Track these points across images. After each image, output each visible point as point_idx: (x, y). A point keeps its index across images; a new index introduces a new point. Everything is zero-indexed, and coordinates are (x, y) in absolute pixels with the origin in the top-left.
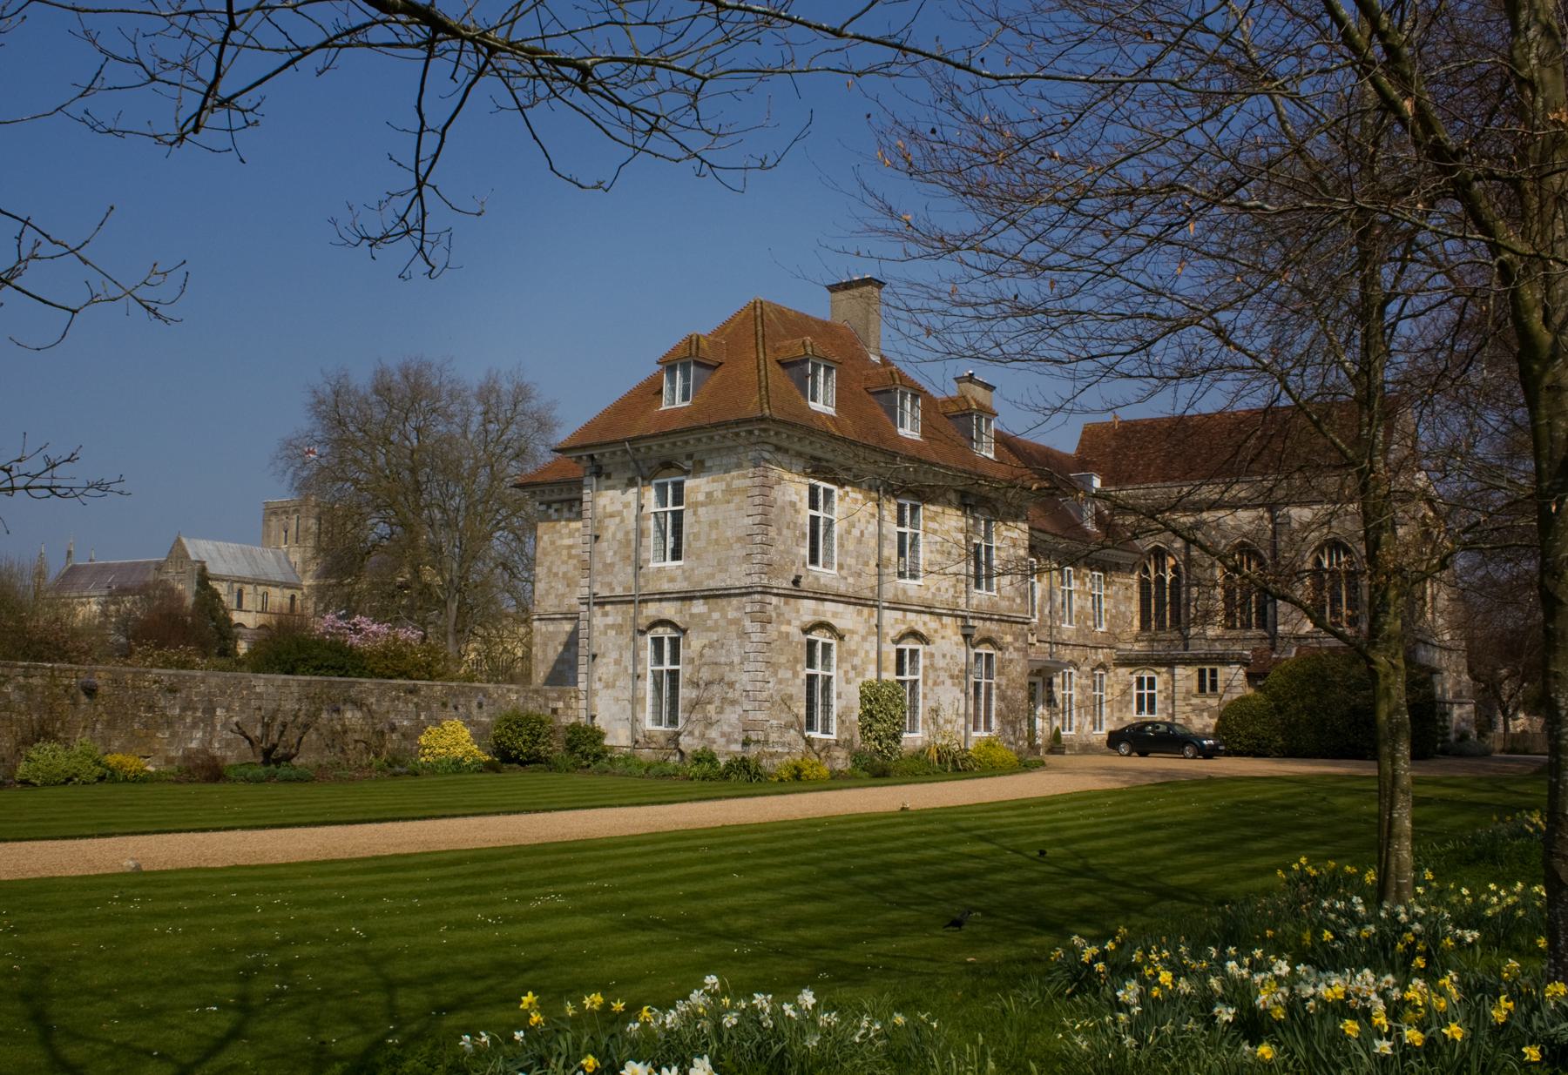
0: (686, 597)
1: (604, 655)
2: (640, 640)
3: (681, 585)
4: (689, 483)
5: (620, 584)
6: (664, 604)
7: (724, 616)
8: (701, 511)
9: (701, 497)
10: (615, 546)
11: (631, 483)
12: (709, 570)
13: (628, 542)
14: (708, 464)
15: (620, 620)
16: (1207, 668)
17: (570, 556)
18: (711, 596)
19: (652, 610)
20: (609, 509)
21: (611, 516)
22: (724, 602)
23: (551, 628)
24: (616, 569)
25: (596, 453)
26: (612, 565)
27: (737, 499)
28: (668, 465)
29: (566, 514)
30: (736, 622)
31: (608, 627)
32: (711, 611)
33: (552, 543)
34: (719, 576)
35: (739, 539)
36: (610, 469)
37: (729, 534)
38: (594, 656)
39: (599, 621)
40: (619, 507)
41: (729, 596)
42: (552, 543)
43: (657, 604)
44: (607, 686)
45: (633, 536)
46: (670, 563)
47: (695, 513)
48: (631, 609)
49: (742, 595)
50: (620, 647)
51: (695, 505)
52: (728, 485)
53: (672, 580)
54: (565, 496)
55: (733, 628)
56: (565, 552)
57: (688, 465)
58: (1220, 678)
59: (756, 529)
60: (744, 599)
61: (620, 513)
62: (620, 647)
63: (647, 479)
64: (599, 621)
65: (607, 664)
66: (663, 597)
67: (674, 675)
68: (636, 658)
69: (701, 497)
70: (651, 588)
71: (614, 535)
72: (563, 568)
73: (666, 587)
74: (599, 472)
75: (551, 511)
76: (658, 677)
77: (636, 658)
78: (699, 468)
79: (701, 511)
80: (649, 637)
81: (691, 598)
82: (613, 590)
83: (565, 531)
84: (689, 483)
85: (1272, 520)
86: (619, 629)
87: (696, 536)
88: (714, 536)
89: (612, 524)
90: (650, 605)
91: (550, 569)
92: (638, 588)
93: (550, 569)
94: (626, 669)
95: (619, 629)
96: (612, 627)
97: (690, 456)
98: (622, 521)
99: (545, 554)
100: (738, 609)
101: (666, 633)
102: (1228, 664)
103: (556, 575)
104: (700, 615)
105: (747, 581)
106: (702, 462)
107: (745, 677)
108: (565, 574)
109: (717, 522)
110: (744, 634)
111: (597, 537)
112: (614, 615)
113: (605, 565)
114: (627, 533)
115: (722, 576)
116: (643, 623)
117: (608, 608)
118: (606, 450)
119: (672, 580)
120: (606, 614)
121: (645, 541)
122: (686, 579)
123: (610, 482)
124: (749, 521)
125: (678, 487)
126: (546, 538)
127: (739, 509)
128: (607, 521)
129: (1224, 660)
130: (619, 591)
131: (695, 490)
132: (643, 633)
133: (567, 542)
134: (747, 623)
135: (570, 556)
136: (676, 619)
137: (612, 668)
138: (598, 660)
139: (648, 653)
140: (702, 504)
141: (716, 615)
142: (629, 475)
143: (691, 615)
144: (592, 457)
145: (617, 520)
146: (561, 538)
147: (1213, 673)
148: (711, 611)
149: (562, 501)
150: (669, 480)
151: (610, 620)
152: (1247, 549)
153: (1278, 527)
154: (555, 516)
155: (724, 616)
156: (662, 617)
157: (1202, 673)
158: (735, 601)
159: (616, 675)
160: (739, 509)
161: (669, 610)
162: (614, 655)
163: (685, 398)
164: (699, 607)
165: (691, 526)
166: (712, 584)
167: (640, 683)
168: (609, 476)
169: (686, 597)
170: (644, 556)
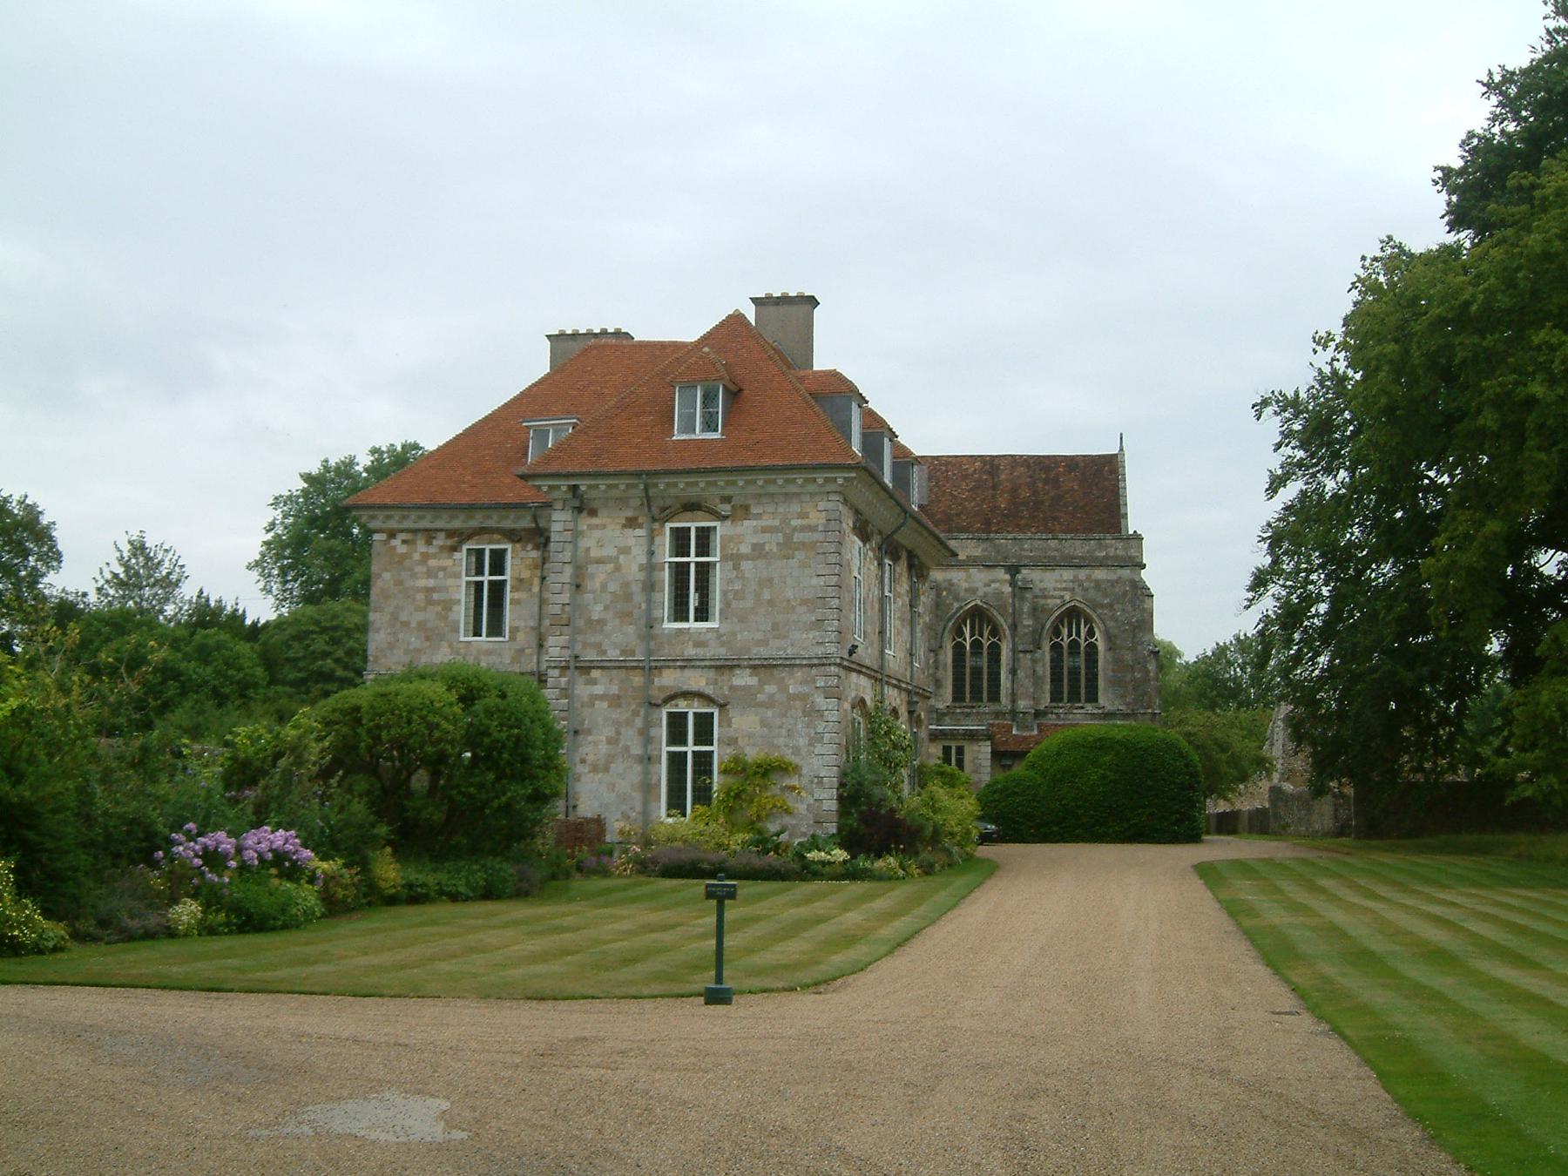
0: (725, 667)
1: (589, 732)
2: (655, 713)
3: (722, 652)
4: (721, 529)
5: (615, 646)
6: (687, 673)
8: (746, 565)
9: (745, 549)
10: (607, 598)
11: (631, 523)
12: (759, 636)
13: (628, 597)
14: (755, 510)
15: (615, 689)
16: (954, 745)
17: (430, 602)
18: (762, 667)
19: (669, 679)
20: (594, 553)
21: (599, 561)
22: (784, 674)
24: (608, 628)
25: (583, 485)
26: (601, 622)
27: (800, 555)
28: (692, 507)
29: (421, 547)
32: (762, 683)
33: (399, 583)
34: (774, 643)
35: (804, 602)
36: (595, 504)
37: (789, 594)
38: (576, 732)
40: (610, 551)
42: (399, 583)
43: (678, 673)
44: (595, 769)
45: (636, 588)
46: (692, 624)
48: (637, 679)
49: (811, 666)
50: (617, 724)
52: (788, 539)
53: (700, 644)
55: (798, 703)
56: (420, 596)
57: (725, 509)
58: (967, 758)
59: (831, 592)
60: (814, 671)
61: (614, 560)
62: (617, 724)
64: (582, 690)
65: (596, 743)
66: (687, 664)
67: (703, 761)
68: (647, 738)
69: (745, 549)
70: (666, 653)
71: (604, 587)
72: (419, 616)
73: (691, 652)
74: (582, 507)
75: (396, 542)
76: (677, 761)
77: (647, 738)
78: (743, 512)
79: (746, 565)
81: (732, 667)
82: (605, 652)
83: (420, 569)
84: (721, 529)
85: (1013, 583)
86: (615, 701)
87: (739, 595)
88: (766, 595)
89: (598, 576)
90: (666, 673)
91: (394, 617)
92: (650, 653)
93: (394, 617)
94: (627, 749)
95: (615, 701)
96: (602, 697)
97: (727, 499)
98: (618, 569)
102: (978, 740)
103: (406, 624)
104: (746, 688)
105: (820, 651)
106: (746, 508)
107: (815, 761)
108: (422, 625)
109: (770, 580)
110: (814, 713)
111: (578, 586)
112: (603, 685)
113: (589, 621)
114: (626, 585)
115: (777, 643)
117: (595, 673)
118: (602, 484)
119: (700, 644)
120: (594, 682)
121: (656, 596)
122: (722, 644)
123: (595, 521)
124: (821, 581)
125: (705, 536)
126: (386, 575)
127: (803, 566)
128: (591, 569)
129: (972, 736)
130: (613, 654)
131: (738, 539)
132: (658, 706)
133: (422, 583)
134: (820, 701)
135: (430, 602)
136: (709, 691)
137: (604, 749)
138: (581, 737)
140: (747, 557)
141: (770, 689)
142: (630, 514)
143: (732, 688)
144: (575, 488)
146: (414, 576)
147: (960, 751)
148: (762, 683)
149: (415, 531)
150: (693, 526)
151: (599, 689)
152: (978, 616)
153: (1020, 590)
154: (402, 549)
155: (783, 688)
156: (685, 688)
157: (947, 750)
158: (799, 674)
159: (610, 758)
160: (803, 566)
161: (697, 680)
162: (609, 731)
163: (709, 425)
164: (743, 679)
165: (730, 582)
166: (764, 652)
167: (653, 768)
168: (593, 513)
170: (657, 613)
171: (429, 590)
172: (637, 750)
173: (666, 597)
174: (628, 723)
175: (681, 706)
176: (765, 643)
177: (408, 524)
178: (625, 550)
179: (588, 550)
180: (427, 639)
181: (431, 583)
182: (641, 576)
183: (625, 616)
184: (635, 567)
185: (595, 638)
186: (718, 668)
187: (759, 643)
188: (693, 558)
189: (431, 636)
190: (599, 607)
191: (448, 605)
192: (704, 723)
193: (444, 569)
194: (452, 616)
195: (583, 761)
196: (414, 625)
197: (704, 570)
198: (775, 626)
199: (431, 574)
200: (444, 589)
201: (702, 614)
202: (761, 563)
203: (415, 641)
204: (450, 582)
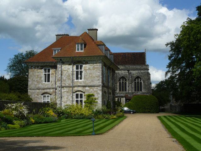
0: (84, 87)
1: (63, 97)
2: (74, 94)
3: (84, 84)
7: (93, 90)
8: (87, 71)
12: (89, 82)
13: (69, 76)
15: (67, 90)
19: (76, 89)
20: (64, 69)
21: (65, 71)
22: (94, 87)
23: (33, 91)
24: (66, 81)
28: (79, 62)
30: (96, 91)
31: (64, 92)
39: (63, 91)
40: (66, 69)
41: (95, 86)
44: (65, 103)
46: (79, 80)
47: (86, 71)
48: (71, 89)
49: (97, 86)
51: (86, 70)
52: (94, 67)
53: (80, 83)
54: (37, 65)
56: (37, 76)
62: (68, 96)
63: (74, 64)
66: (79, 86)
69: (87, 68)
71: (66, 75)
72: (36, 79)
73: (79, 84)
79: (87, 71)
80: (75, 94)
83: (36, 72)
84: (84, 66)
86: (68, 92)
89: (65, 73)
94: (69, 99)
95: (68, 92)
96: (65, 92)
97: (84, 61)
98: (68, 72)
99: (31, 76)
100: (96, 89)
101: (79, 93)
103: (34, 80)
104: (87, 90)
105: (99, 84)
106: (87, 62)
112: (65, 90)
116: (74, 91)
117: (64, 88)
119: (80, 83)
120: (64, 89)
121: (74, 76)
129: (122, 97)
130: (67, 85)
132: (74, 93)
133: (37, 74)
134: (99, 92)
136: (82, 90)
137: (66, 99)
139: (75, 97)
141: (91, 90)
144: (61, 59)
145: (66, 71)
146: (36, 73)
147: (120, 99)
151: (65, 90)
152: (123, 78)
155: (93, 90)
156: (78, 90)
158: (96, 87)
159: (67, 101)
160: (96, 71)
161: (80, 89)
162: (67, 97)
163: (82, 49)
164: (87, 88)
169: (84, 87)
170: (74, 78)
171: (38, 75)
172: (71, 99)
173: (75, 76)
174: (70, 95)
175: (78, 93)
176: (90, 83)
177: (34, 65)
178: (69, 69)
179: (63, 69)
180: (38, 83)
181: (38, 74)
182: (72, 73)
183: (69, 79)
184: (70, 71)
185: (65, 82)
186: (83, 87)
187: (89, 83)
188: (79, 70)
189: (38, 82)
190: (65, 78)
191: (41, 77)
192: (81, 95)
193: (40, 72)
194: (42, 79)
195: (63, 101)
196: (35, 81)
197: (81, 72)
198: (92, 80)
199: (38, 73)
200: (40, 75)
201: (81, 79)
202: (90, 71)
203: (36, 83)
204: (41, 74)
